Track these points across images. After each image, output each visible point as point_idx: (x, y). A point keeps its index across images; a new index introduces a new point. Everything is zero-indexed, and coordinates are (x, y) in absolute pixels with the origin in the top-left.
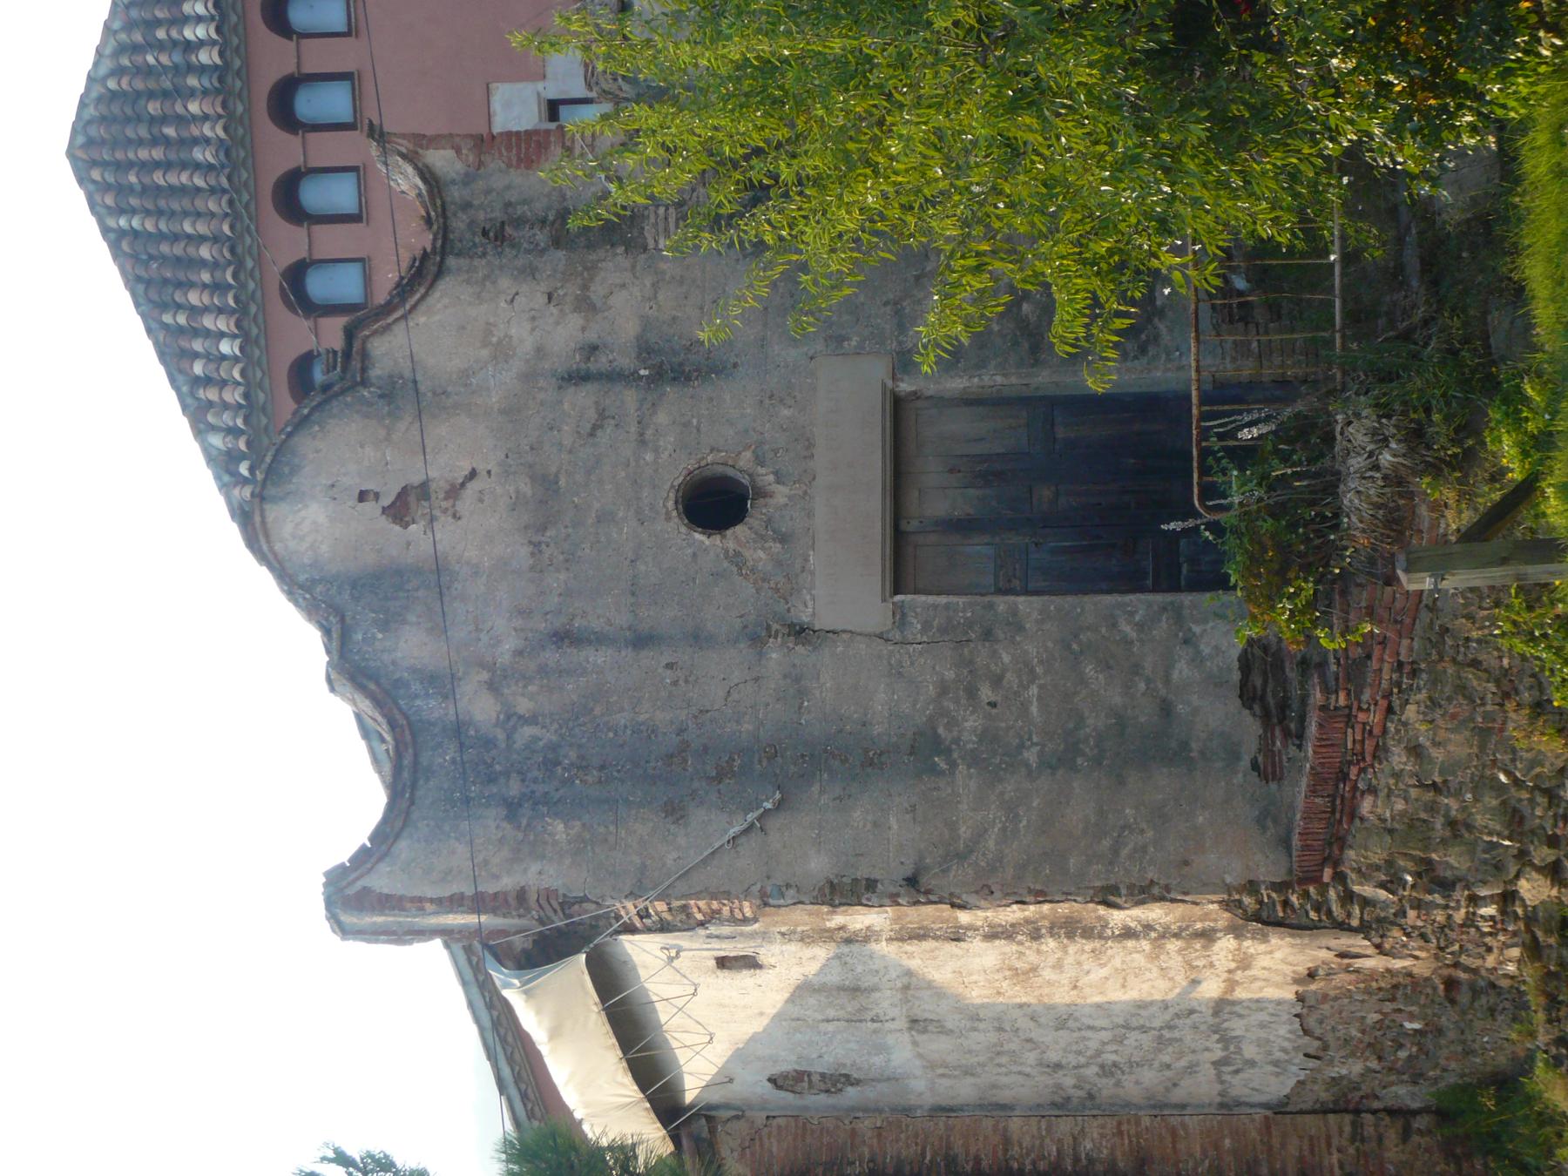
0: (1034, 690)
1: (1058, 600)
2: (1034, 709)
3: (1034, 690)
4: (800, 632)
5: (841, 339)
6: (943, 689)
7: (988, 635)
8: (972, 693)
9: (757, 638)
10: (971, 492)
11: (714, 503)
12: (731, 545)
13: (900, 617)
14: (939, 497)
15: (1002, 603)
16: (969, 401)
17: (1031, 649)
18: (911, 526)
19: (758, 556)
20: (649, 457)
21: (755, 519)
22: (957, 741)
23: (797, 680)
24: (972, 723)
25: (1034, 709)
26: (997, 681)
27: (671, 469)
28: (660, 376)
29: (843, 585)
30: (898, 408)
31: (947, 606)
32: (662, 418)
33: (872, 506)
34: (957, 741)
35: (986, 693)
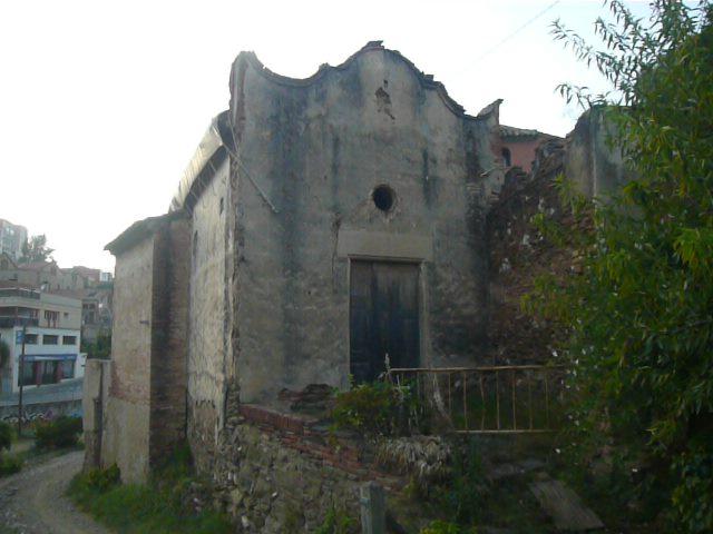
0: (315, 308)
1: (348, 318)
2: (309, 308)
3: (315, 308)
4: (337, 224)
5: (439, 245)
6: (316, 275)
7: (335, 292)
8: (315, 285)
9: (335, 209)
10: (386, 290)
11: (383, 198)
12: (368, 202)
13: (342, 260)
14: (384, 277)
15: (347, 298)
16: (417, 289)
17: (330, 308)
18: (375, 267)
19: (365, 211)
20: (399, 177)
21: (377, 211)
22: (296, 279)
23: (320, 222)
24: (303, 285)
25: (309, 308)
26: (317, 294)
27: (397, 185)
28: (426, 183)
29: (353, 241)
30: (416, 264)
31: (346, 278)
32: (412, 183)
33: (383, 253)
34: (296, 279)
35: (314, 290)
